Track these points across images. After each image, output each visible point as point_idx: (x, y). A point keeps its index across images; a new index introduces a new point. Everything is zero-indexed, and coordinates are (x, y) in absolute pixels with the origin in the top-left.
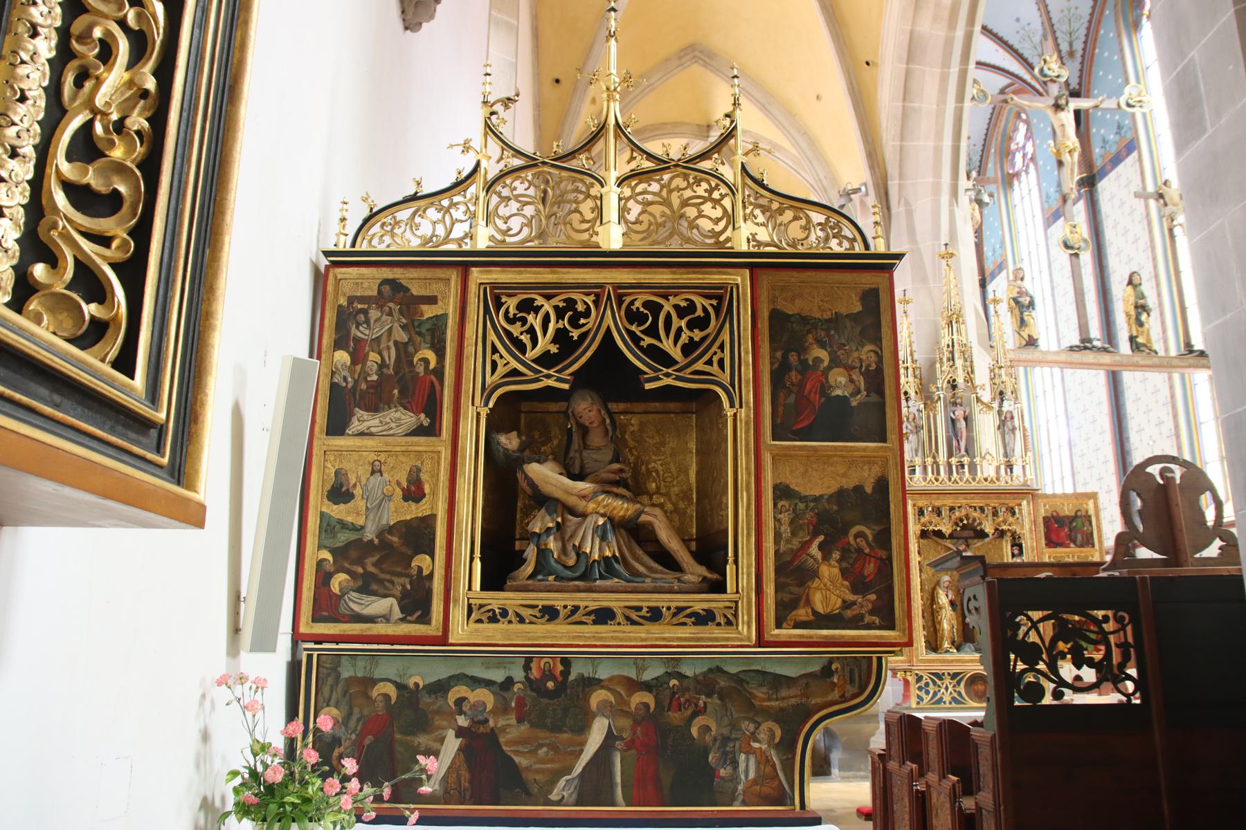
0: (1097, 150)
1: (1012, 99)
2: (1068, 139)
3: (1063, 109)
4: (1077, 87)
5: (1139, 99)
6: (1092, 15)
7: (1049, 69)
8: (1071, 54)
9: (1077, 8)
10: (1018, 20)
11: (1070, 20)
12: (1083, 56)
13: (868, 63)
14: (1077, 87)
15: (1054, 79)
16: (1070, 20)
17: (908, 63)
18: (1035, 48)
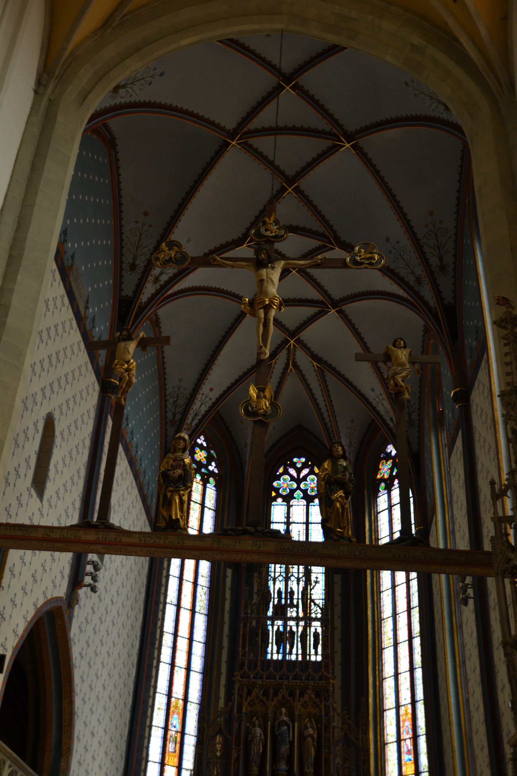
0: (468, 362)
1: (215, 260)
2: (266, 294)
3: (266, 266)
4: (453, 301)
5: (369, 255)
6: (456, 227)
7: (266, 230)
8: (443, 268)
9: (441, 222)
10: (388, 240)
11: (436, 234)
12: (454, 270)
14: (453, 301)
15: (272, 239)
16: (436, 234)
18: (408, 265)
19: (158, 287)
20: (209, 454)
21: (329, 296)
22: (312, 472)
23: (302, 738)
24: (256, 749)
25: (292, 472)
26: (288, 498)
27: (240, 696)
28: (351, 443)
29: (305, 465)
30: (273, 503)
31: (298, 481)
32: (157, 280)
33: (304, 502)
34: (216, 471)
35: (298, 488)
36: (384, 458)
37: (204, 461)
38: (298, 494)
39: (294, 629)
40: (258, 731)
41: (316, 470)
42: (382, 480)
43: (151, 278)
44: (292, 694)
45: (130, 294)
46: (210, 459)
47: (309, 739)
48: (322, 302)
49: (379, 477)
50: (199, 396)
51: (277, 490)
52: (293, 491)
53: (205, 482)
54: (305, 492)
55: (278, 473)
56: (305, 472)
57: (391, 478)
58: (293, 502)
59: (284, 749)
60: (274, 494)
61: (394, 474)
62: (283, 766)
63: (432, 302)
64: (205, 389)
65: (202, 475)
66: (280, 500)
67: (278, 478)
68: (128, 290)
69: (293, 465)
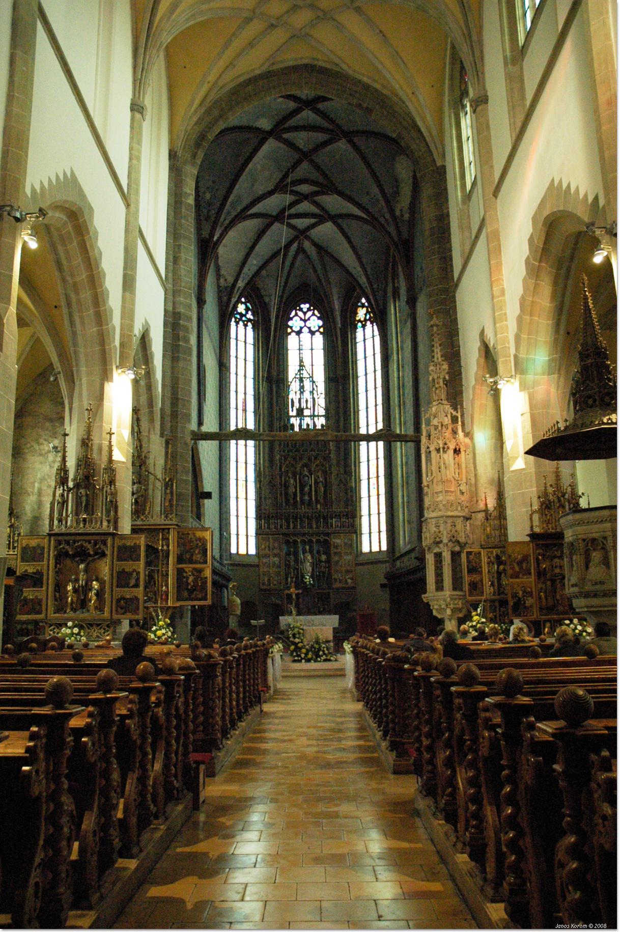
13: (56, 307)
17: (69, 308)
19: (223, 228)
20: (246, 306)
21: (326, 211)
22: (314, 314)
23: (316, 483)
24: (291, 490)
25: (300, 314)
26: (299, 333)
27: (281, 463)
28: (339, 297)
29: (309, 310)
30: (289, 337)
31: (305, 321)
32: (222, 223)
33: (309, 335)
34: (252, 318)
35: (305, 326)
36: (360, 306)
37: (244, 312)
38: (305, 330)
39: (309, 423)
40: (292, 481)
41: (316, 312)
42: (360, 321)
43: (219, 224)
44: (310, 459)
45: (207, 236)
46: (247, 309)
47: (321, 484)
48: (322, 216)
49: (357, 319)
50: (242, 275)
51: (291, 328)
52: (301, 328)
53: (246, 326)
54: (309, 328)
55: (291, 316)
56: (309, 314)
57: (365, 320)
58: (301, 335)
59: (307, 489)
60: (289, 330)
61: (368, 317)
62: (306, 498)
63: (396, 238)
64: (245, 270)
65: (243, 321)
66: (293, 334)
67: (291, 319)
68: (205, 234)
69: (301, 310)
